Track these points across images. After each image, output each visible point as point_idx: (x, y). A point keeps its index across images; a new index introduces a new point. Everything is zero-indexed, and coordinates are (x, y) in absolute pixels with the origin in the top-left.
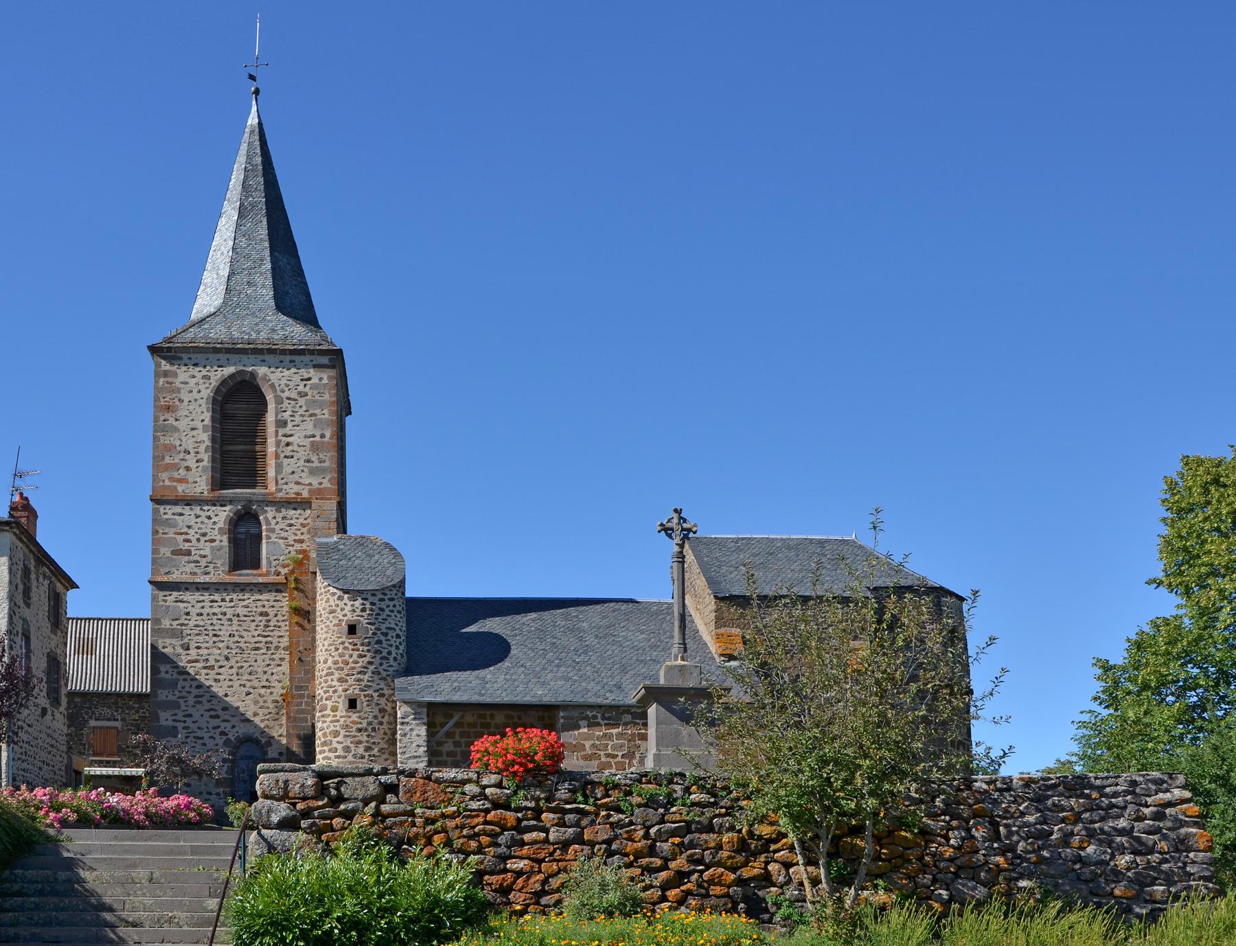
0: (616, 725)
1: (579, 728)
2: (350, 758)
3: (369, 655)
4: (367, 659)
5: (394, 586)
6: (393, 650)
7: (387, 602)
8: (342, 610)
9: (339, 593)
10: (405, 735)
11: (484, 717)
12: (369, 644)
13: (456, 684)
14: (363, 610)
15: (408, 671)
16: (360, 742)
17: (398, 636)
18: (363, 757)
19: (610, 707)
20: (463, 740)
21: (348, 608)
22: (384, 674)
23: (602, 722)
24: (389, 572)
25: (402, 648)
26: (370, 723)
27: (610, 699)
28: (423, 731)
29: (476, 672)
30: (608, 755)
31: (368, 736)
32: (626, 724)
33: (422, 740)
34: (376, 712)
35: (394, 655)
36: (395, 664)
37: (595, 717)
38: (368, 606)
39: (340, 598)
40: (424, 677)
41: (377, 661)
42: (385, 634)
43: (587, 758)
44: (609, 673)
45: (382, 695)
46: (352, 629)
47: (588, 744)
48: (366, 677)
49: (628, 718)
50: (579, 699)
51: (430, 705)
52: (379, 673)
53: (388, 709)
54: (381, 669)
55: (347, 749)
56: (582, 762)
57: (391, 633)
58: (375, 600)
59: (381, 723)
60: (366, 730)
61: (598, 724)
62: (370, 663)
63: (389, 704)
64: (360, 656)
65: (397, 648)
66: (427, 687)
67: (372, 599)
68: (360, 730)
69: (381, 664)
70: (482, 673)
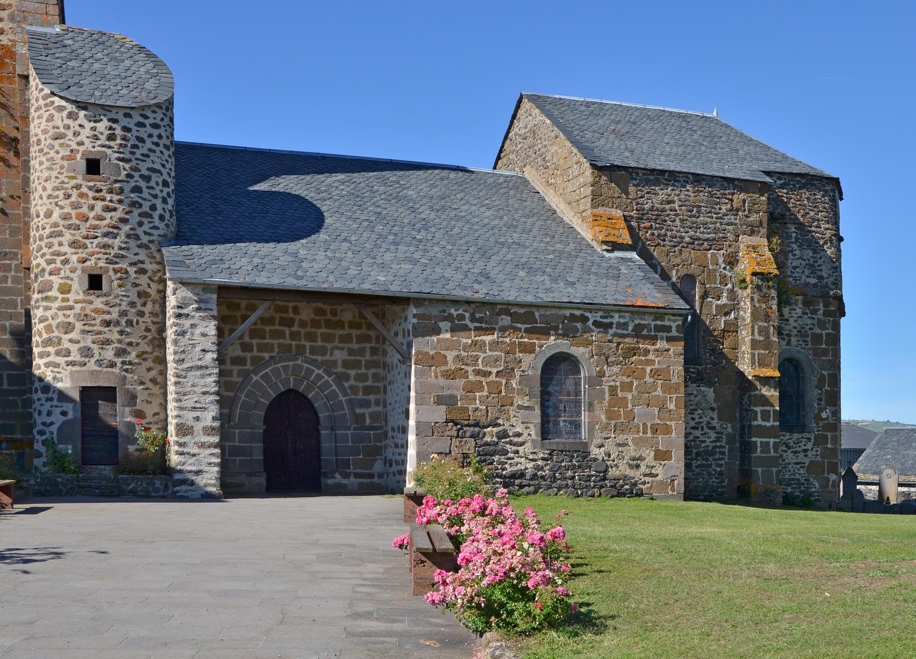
0: (490, 331)
1: (438, 332)
2: (92, 365)
3: (121, 207)
4: (119, 214)
5: (158, 106)
6: (158, 203)
7: (149, 129)
8: (76, 134)
9: (70, 107)
10: (183, 333)
11: (284, 310)
12: (121, 191)
13: (256, 260)
14: (111, 137)
15: (180, 238)
16: (108, 342)
17: (165, 184)
18: (112, 365)
19: (484, 304)
20: (254, 342)
21: (86, 132)
22: (145, 239)
23: (471, 325)
24: (150, 85)
25: (171, 201)
26: (123, 314)
27: (481, 292)
28: (211, 328)
29: (283, 246)
30: (478, 373)
31: (121, 333)
32: (503, 329)
33: (209, 343)
34: (134, 297)
35: (159, 211)
36: (162, 225)
37: (461, 317)
38: (119, 132)
39: (71, 115)
40: (207, 248)
41: (134, 218)
42: (147, 179)
43: (450, 375)
44: (467, 257)
45: (142, 271)
46: (93, 167)
47: (450, 356)
48: (117, 242)
49: (506, 320)
50: (438, 290)
51: (223, 290)
52: (137, 237)
53: (153, 291)
54: (140, 231)
55: (86, 352)
56: (442, 381)
57: (155, 178)
58: (130, 123)
59: (141, 314)
60: (118, 323)
61: (466, 328)
62: (124, 221)
63: (154, 286)
64: (107, 209)
65: (165, 201)
66: (214, 262)
67: (125, 122)
68: (107, 323)
69: (140, 224)
70: (293, 246)
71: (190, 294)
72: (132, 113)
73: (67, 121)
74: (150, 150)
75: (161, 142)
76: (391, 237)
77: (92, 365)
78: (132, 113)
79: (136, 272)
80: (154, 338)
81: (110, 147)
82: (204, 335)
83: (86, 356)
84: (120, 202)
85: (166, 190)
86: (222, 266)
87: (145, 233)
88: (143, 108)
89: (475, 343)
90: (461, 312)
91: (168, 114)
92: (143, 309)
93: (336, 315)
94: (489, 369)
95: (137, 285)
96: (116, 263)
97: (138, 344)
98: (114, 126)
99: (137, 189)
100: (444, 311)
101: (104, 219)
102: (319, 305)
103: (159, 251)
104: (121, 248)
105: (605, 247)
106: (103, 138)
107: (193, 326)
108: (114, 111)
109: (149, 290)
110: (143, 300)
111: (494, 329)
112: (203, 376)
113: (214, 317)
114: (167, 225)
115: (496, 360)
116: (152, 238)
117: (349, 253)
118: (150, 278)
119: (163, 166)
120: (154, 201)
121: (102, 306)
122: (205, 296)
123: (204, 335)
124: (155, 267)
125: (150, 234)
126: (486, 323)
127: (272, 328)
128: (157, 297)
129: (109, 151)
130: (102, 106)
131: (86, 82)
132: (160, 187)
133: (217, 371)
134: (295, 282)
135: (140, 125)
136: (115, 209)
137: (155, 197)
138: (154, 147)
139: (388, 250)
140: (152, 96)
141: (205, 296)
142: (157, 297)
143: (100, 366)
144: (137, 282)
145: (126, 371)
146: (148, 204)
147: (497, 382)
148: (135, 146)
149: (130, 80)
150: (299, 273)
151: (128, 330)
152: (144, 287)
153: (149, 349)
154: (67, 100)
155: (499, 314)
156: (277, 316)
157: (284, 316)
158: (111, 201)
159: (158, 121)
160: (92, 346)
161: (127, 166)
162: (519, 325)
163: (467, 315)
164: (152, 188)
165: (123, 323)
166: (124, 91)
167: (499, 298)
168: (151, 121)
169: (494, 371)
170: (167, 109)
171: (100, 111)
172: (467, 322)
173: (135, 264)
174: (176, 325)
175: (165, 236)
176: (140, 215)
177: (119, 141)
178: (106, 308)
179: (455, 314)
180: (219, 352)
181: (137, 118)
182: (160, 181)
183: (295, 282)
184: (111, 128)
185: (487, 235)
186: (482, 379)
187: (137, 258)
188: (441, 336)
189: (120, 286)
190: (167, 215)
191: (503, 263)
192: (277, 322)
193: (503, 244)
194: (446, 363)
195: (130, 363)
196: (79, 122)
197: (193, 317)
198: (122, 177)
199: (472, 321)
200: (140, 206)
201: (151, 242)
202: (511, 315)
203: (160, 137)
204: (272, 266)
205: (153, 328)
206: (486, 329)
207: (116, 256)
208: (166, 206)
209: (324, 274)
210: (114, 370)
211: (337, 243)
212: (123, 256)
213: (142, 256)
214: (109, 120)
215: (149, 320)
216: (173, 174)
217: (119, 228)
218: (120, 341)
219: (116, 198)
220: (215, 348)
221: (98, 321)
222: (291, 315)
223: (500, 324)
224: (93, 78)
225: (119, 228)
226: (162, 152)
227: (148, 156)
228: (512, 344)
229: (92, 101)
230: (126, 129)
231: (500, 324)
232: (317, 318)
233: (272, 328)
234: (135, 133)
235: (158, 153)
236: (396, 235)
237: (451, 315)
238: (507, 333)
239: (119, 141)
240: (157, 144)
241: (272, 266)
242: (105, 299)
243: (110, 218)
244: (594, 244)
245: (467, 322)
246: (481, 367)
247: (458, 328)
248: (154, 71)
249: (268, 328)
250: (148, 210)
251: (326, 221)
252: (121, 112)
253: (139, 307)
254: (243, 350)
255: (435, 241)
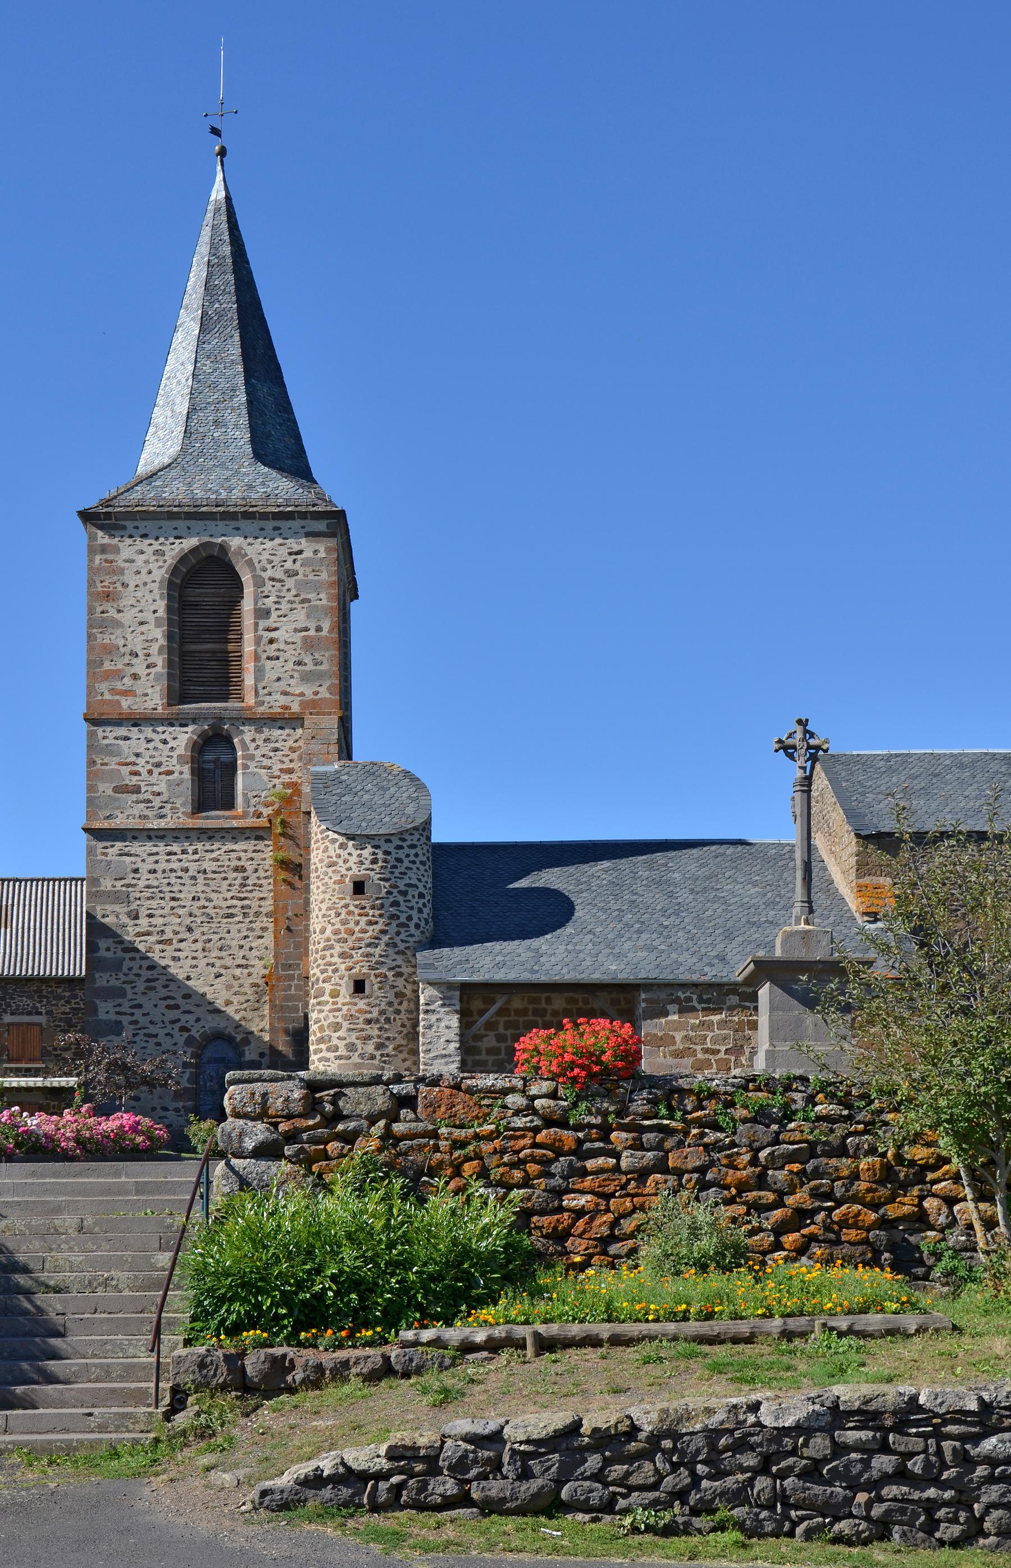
0: (718, 1010)
1: (666, 1014)
2: (356, 1059)
3: (381, 921)
4: (380, 926)
5: (416, 828)
6: (414, 913)
7: (407, 850)
8: (345, 861)
9: (341, 839)
10: (430, 1027)
11: (538, 1001)
12: (382, 906)
13: (499, 958)
14: (374, 861)
15: (435, 942)
16: (369, 1038)
17: (421, 896)
18: (373, 1057)
19: (710, 986)
20: (508, 1032)
21: (354, 859)
22: (402, 946)
23: (699, 1007)
24: (409, 810)
25: (426, 911)
26: (382, 1012)
27: (711, 974)
28: (454, 1021)
29: (527, 942)
30: (706, 1051)
31: (380, 1029)
32: (731, 1009)
33: (453, 1034)
34: (391, 996)
35: (415, 920)
36: (418, 933)
37: (689, 999)
38: (380, 856)
39: (343, 846)
40: (457, 950)
41: (393, 928)
42: (404, 893)
43: (678, 1054)
44: (709, 941)
45: (399, 975)
46: (359, 888)
47: (678, 1036)
48: (378, 951)
49: (734, 1000)
50: (667, 976)
51: (465, 987)
52: (395, 945)
53: (408, 992)
54: (397, 940)
55: (351, 1047)
56: (670, 1061)
57: (412, 892)
58: (390, 847)
59: (398, 1012)
60: (378, 1021)
61: (693, 1009)
62: (383, 932)
63: (409, 987)
64: (370, 923)
65: (420, 911)
66: (460, 963)
67: (385, 847)
68: (369, 1022)
69: (398, 933)
70: (535, 943)
71: (436, 993)
72: (392, 838)
73: (338, 851)
74: (407, 868)
75: (417, 860)
76: (637, 926)
77: (356, 1059)
78: (392, 838)
79: (393, 976)
80: (409, 1033)
81: (373, 870)
82: (448, 1027)
83: (351, 1051)
84: (381, 916)
85: (422, 901)
86: (467, 966)
87: (402, 941)
88: (401, 833)
89: (703, 1023)
90: (688, 994)
91: (425, 834)
92: (400, 1007)
93: (588, 1003)
94: (718, 1047)
95: (394, 987)
96: (377, 969)
97: (394, 1038)
98: (376, 851)
99: (395, 904)
100: (672, 994)
101: (366, 932)
102: (571, 994)
103: (414, 955)
104: (381, 956)
105: (866, 918)
106: (367, 862)
107: (439, 1020)
108: (377, 838)
109: (405, 991)
110: (399, 1000)
111: (722, 1009)
112: (447, 1064)
113: (456, 1012)
114: (422, 932)
115: (725, 1039)
116: (408, 945)
117: (590, 945)
118: (406, 980)
119: (419, 880)
120: (411, 912)
121: (364, 1007)
122: (449, 994)
123: (448, 1027)
124: (411, 970)
125: (406, 942)
126: (714, 1003)
127: (526, 1018)
128: (412, 997)
129: (372, 873)
130: (368, 836)
131: (355, 814)
132: (416, 899)
133: (459, 1058)
134: (530, 976)
135: (399, 847)
136: (376, 923)
137: (412, 908)
138: (411, 865)
139: (630, 939)
140: (410, 820)
141: (449, 994)
142: (412, 997)
143: (363, 1058)
144: (395, 984)
145: (385, 1062)
146: (405, 915)
147: (725, 1059)
148: (394, 867)
149: (393, 807)
150: (536, 968)
151: (386, 1026)
152: (401, 988)
153: (404, 1042)
154: (339, 833)
155: (727, 994)
156: (531, 1007)
157: (537, 1006)
158: (373, 916)
159: (415, 842)
160: (356, 1042)
161: (387, 885)
162: (748, 1004)
163: (695, 997)
164: (409, 901)
165: (382, 1020)
166: (387, 819)
167: (725, 980)
168: (409, 843)
169: (723, 1048)
170: (424, 830)
171: (366, 840)
172: (695, 1003)
173: (393, 968)
174: (424, 1020)
175: (420, 942)
176: (397, 926)
177: (380, 864)
178: (368, 1008)
179: (682, 997)
180: (461, 1041)
181: (397, 842)
182: (416, 894)
183: (530, 976)
184: (374, 854)
185: (740, 916)
186: (711, 1057)
187: (395, 963)
188: (670, 1018)
189: (380, 989)
190: (422, 924)
191: (745, 943)
192: (530, 1013)
193: (754, 923)
194: (674, 1043)
195: (388, 1055)
196: (348, 851)
197: (439, 1012)
198: (383, 894)
199: (699, 1003)
200: (398, 917)
201: (407, 948)
202: (739, 994)
203: (416, 855)
204: (513, 963)
205: (408, 1024)
206: (714, 1009)
207: (377, 963)
208: (421, 916)
209: (559, 967)
210: (374, 1062)
211: (581, 936)
212: (383, 963)
213: (399, 962)
214: (373, 847)
215: (404, 1017)
216: (430, 885)
217: (380, 939)
218: (379, 1037)
219: (377, 912)
220: (457, 1038)
221: (361, 1020)
222: (544, 1005)
223: (728, 1004)
224: (362, 810)
225: (380, 939)
226: (418, 869)
227: (405, 874)
228: (741, 1022)
229: (359, 833)
230: (387, 853)
231: (728, 1004)
232: (569, 1007)
233: (526, 1018)
234: (394, 855)
235: (415, 870)
236: (643, 923)
237: (678, 997)
238: (735, 1012)
239: (380, 864)
240: (414, 862)
241: (513, 963)
242: (367, 1000)
243: (373, 930)
244: (857, 915)
245: (695, 1003)
246: (709, 1045)
247: (685, 1009)
248: (415, 795)
249: (521, 1019)
250: (404, 920)
251: (576, 914)
252: (383, 839)
253: (396, 1006)
254: (498, 1041)
255: (681, 926)
